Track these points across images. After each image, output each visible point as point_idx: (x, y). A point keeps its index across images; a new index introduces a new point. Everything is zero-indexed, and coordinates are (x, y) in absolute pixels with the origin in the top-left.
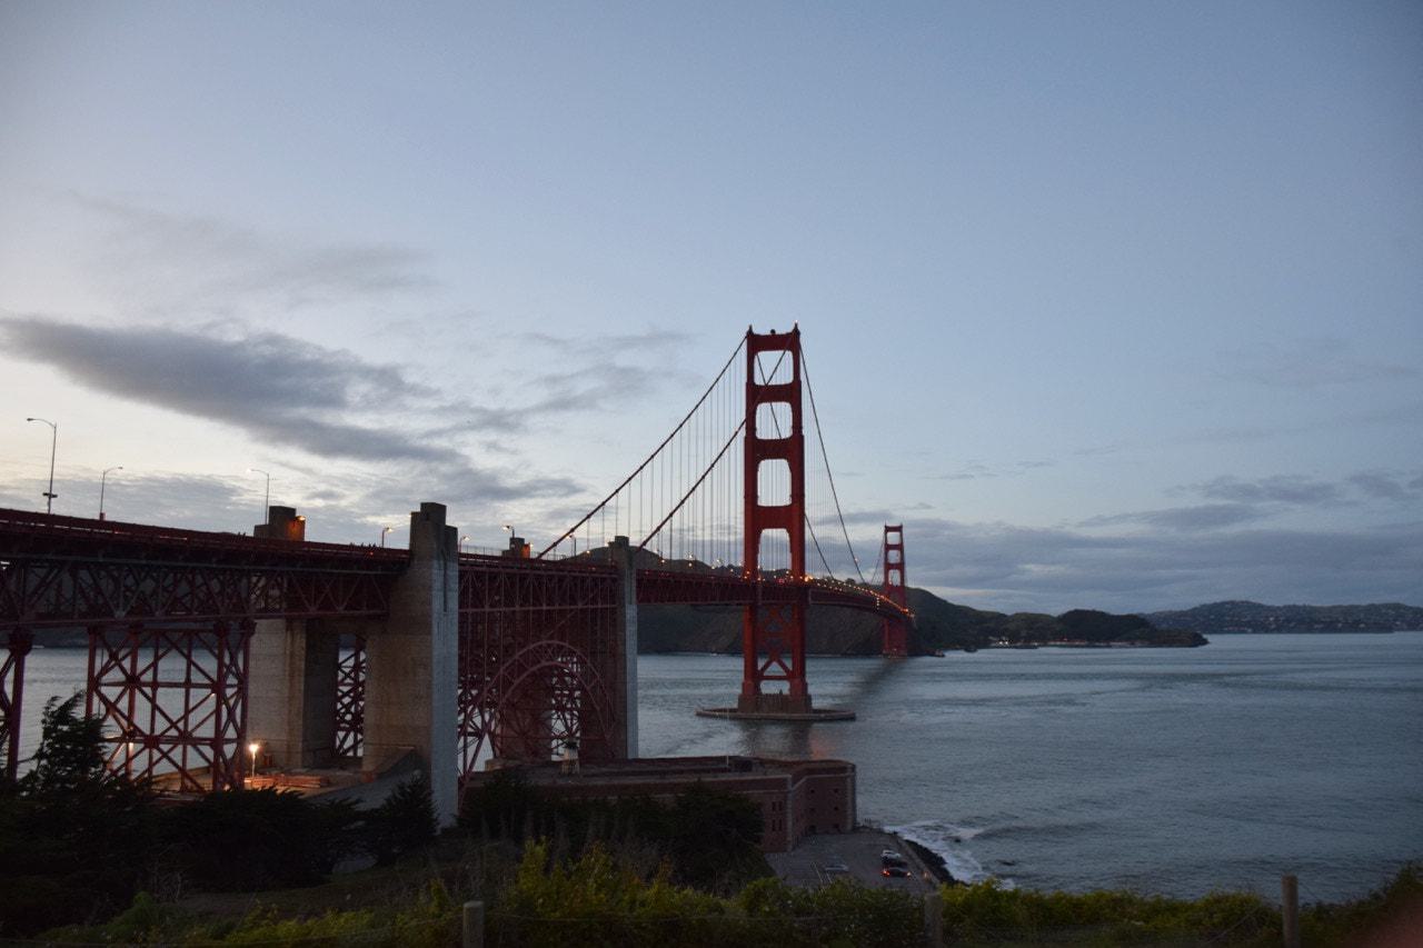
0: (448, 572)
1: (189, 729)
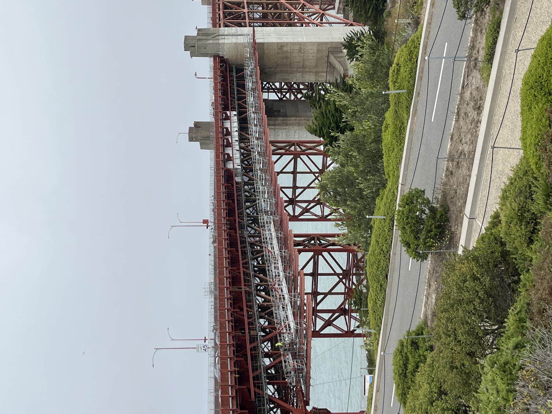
1: (318, 171)
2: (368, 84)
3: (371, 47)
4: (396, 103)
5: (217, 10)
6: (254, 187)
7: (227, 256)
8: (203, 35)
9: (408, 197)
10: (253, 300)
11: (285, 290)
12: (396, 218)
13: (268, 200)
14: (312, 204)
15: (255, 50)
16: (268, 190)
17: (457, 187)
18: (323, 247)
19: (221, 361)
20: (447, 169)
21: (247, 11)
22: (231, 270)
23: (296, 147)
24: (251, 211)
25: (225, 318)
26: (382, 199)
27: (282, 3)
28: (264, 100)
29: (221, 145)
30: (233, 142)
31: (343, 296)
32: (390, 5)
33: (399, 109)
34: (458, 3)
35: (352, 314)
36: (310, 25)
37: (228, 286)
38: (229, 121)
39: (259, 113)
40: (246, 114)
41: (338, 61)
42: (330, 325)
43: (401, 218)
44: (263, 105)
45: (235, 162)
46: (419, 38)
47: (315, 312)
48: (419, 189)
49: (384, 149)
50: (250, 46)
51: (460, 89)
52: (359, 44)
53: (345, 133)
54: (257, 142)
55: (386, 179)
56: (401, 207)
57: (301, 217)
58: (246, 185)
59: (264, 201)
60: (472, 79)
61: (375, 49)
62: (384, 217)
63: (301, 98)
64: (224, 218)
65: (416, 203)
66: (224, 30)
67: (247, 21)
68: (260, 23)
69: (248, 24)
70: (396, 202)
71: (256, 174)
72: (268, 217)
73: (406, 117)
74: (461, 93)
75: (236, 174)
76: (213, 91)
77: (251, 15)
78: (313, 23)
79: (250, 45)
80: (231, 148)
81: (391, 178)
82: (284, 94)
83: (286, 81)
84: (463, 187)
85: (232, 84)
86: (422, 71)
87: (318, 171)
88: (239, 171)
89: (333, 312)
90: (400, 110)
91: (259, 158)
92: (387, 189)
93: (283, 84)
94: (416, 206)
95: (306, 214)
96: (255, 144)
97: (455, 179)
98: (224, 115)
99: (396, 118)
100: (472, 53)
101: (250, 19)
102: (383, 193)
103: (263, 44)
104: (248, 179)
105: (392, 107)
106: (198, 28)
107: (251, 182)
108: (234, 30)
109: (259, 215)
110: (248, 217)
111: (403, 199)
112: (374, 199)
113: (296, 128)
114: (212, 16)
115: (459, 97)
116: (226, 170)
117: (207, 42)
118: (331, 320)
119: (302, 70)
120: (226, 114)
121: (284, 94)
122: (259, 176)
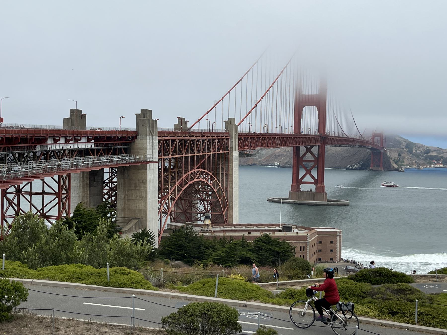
0: (153, 141)
1: (45, 212)
2: (114, 250)
3: (142, 251)
4: (99, 273)
5: (171, 135)
6: (31, 160)
8: (153, 124)
9: (21, 288)
12: (2, 278)
13: (20, 172)
14: (16, 208)
15: (141, 163)
16: (29, 172)
17: (29, 328)
20: (44, 318)
21: (170, 157)
23: (65, 194)
24: (11, 158)
26: (20, 266)
27: (176, 183)
28: (103, 170)
30: (70, 144)
32: (174, 263)
33: (94, 276)
34: (174, 317)
36: (160, 204)
38: (86, 142)
39: (93, 165)
40: (92, 155)
41: (133, 226)
43: (2, 283)
44: (99, 168)
45: (52, 145)
46: (149, 288)
48: (28, 297)
49: (62, 266)
50: (144, 159)
51: (109, 323)
52: (145, 242)
53: (75, 234)
54: (70, 163)
55: (37, 268)
56: (12, 283)
58: (33, 154)
59: (19, 169)
60: (117, 331)
61: (140, 254)
62: (3, 269)
63: (105, 198)
64: (4, 135)
65: (15, 295)
67: (163, 157)
68: (161, 167)
69: (161, 158)
70: (17, 278)
71: (42, 162)
72: (5, 171)
73: (88, 282)
74: (106, 324)
75: (42, 146)
76: (110, 130)
77: (167, 160)
78: (161, 206)
79: (145, 159)
80: (64, 142)
81: (38, 273)
82: (108, 185)
83: (117, 186)
84: (29, 332)
85: (116, 145)
86: (124, 292)
87: (45, 212)
88: (45, 149)
90: (93, 277)
91: (56, 165)
92: (29, 270)
93: (116, 184)
94: (12, 295)
95: (8, 202)
96: (68, 162)
97: (36, 325)
98: (91, 138)
99: (87, 274)
100: (137, 330)
101: (164, 159)
102: (25, 266)
104: (39, 155)
105: (95, 270)
106: (158, 120)
107: (36, 158)
108: (156, 147)
109: (6, 164)
110: (5, 155)
111: (19, 284)
112: (19, 260)
113: (81, 194)
114: (166, 131)
115: (103, 323)
117: (147, 127)
120: (92, 139)
121: (108, 185)
122: (41, 164)
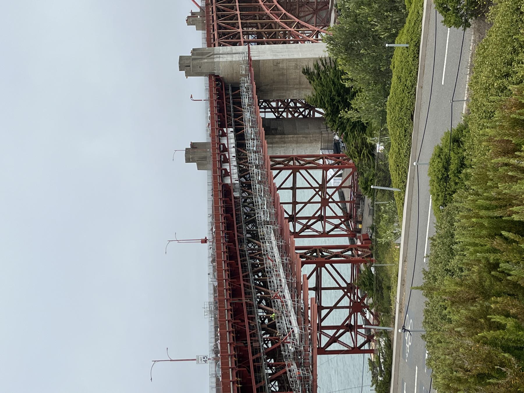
0: (220, 53)
1: (318, 186)
5: (212, 30)
7: (227, 268)
8: (198, 54)
10: (254, 311)
11: (288, 296)
18: (326, 259)
19: (222, 372)
22: (231, 282)
25: (226, 329)
27: (276, 22)
29: (220, 191)
31: (348, 309)
35: (358, 330)
37: (229, 298)
42: (335, 342)
47: (320, 328)
57: (302, 234)
66: (219, 49)
85: (228, 102)
87: (318, 186)
89: (338, 328)
95: (307, 230)
98: (221, 132)
103: (258, 61)
108: (229, 48)
116: (224, 185)
117: (202, 61)
118: (336, 336)
119: (298, 86)
120: (223, 131)
